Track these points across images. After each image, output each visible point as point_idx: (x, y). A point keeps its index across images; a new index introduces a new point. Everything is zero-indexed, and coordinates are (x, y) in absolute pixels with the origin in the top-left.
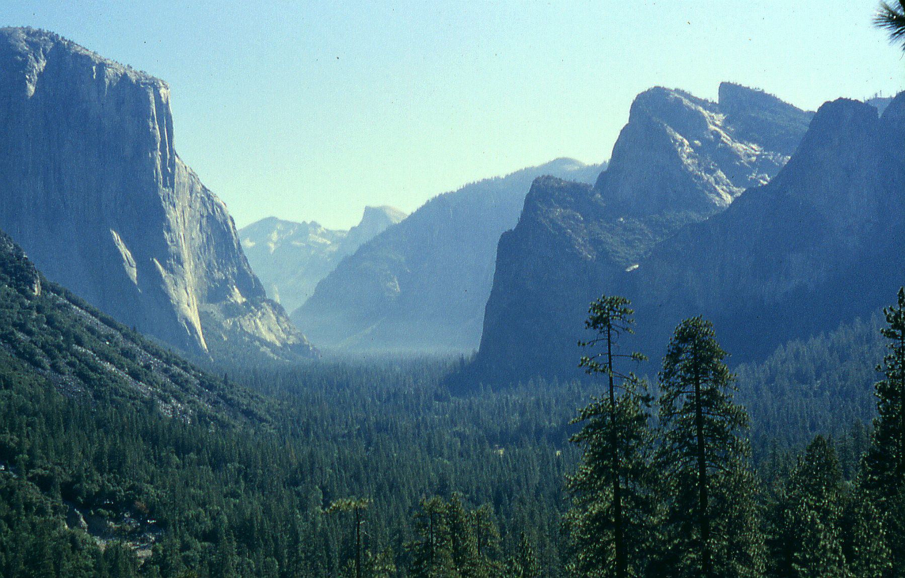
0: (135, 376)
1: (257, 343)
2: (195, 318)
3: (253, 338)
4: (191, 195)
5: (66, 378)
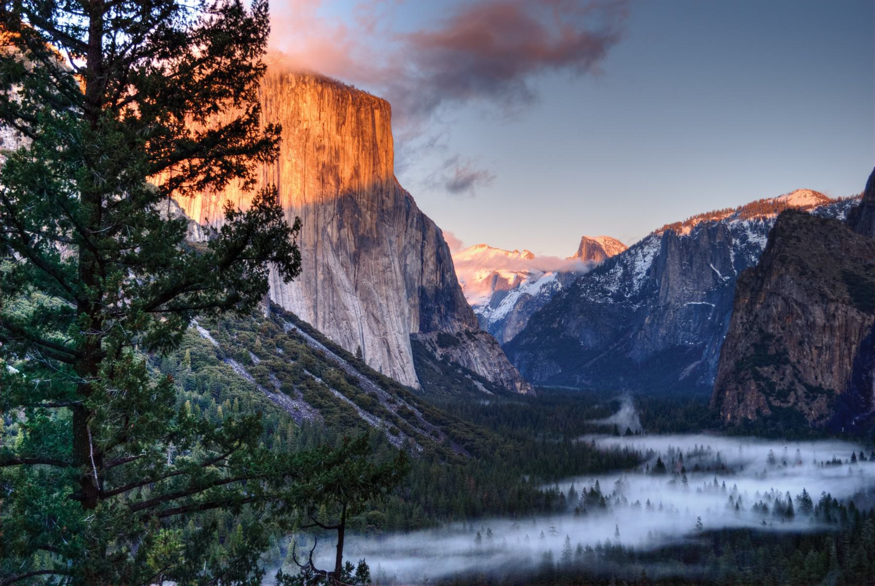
0: (362, 405)
1: (469, 377)
2: (406, 347)
3: (467, 371)
4: (407, 220)
5: (295, 404)
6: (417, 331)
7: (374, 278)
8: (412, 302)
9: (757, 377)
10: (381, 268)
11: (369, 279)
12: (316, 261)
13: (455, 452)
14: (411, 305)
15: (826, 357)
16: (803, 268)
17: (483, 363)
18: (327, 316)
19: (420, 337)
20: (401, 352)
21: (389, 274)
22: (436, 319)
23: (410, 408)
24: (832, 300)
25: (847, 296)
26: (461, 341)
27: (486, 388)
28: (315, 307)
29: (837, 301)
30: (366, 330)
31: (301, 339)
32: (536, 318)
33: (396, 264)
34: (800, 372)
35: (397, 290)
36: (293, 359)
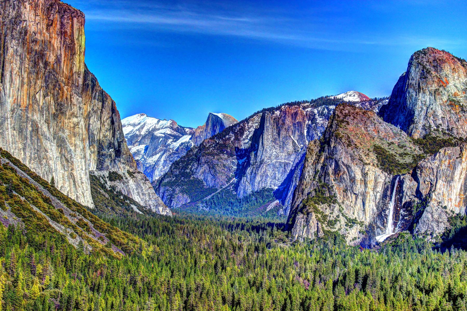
1: (128, 202)
2: (86, 179)
3: (126, 198)
6: (95, 170)
7: (67, 132)
8: (92, 150)
9: (317, 211)
10: (72, 125)
11: (63, 132)
12: (27, 117)
13: (113, 251)
14: (91, 151)
15: (359, 201)
16: (349, 142)
17: (138, 193)
18: (33, 156)
19: (96, 174)
20: (82, 183)
21: (77, 130)
22: (107, 162)
23: (85, 221)
24: (366, 164)
25: (376, 162)
26: (124, 178)
27: (139, 210)
28: (24, 149)
29: (369, 164)
30: (59, 167)
31: (12, 169)
32: (176, 164)
33: (82, 123)
34: (343, 209)
35: (83, 140)
36: (5, 183)
